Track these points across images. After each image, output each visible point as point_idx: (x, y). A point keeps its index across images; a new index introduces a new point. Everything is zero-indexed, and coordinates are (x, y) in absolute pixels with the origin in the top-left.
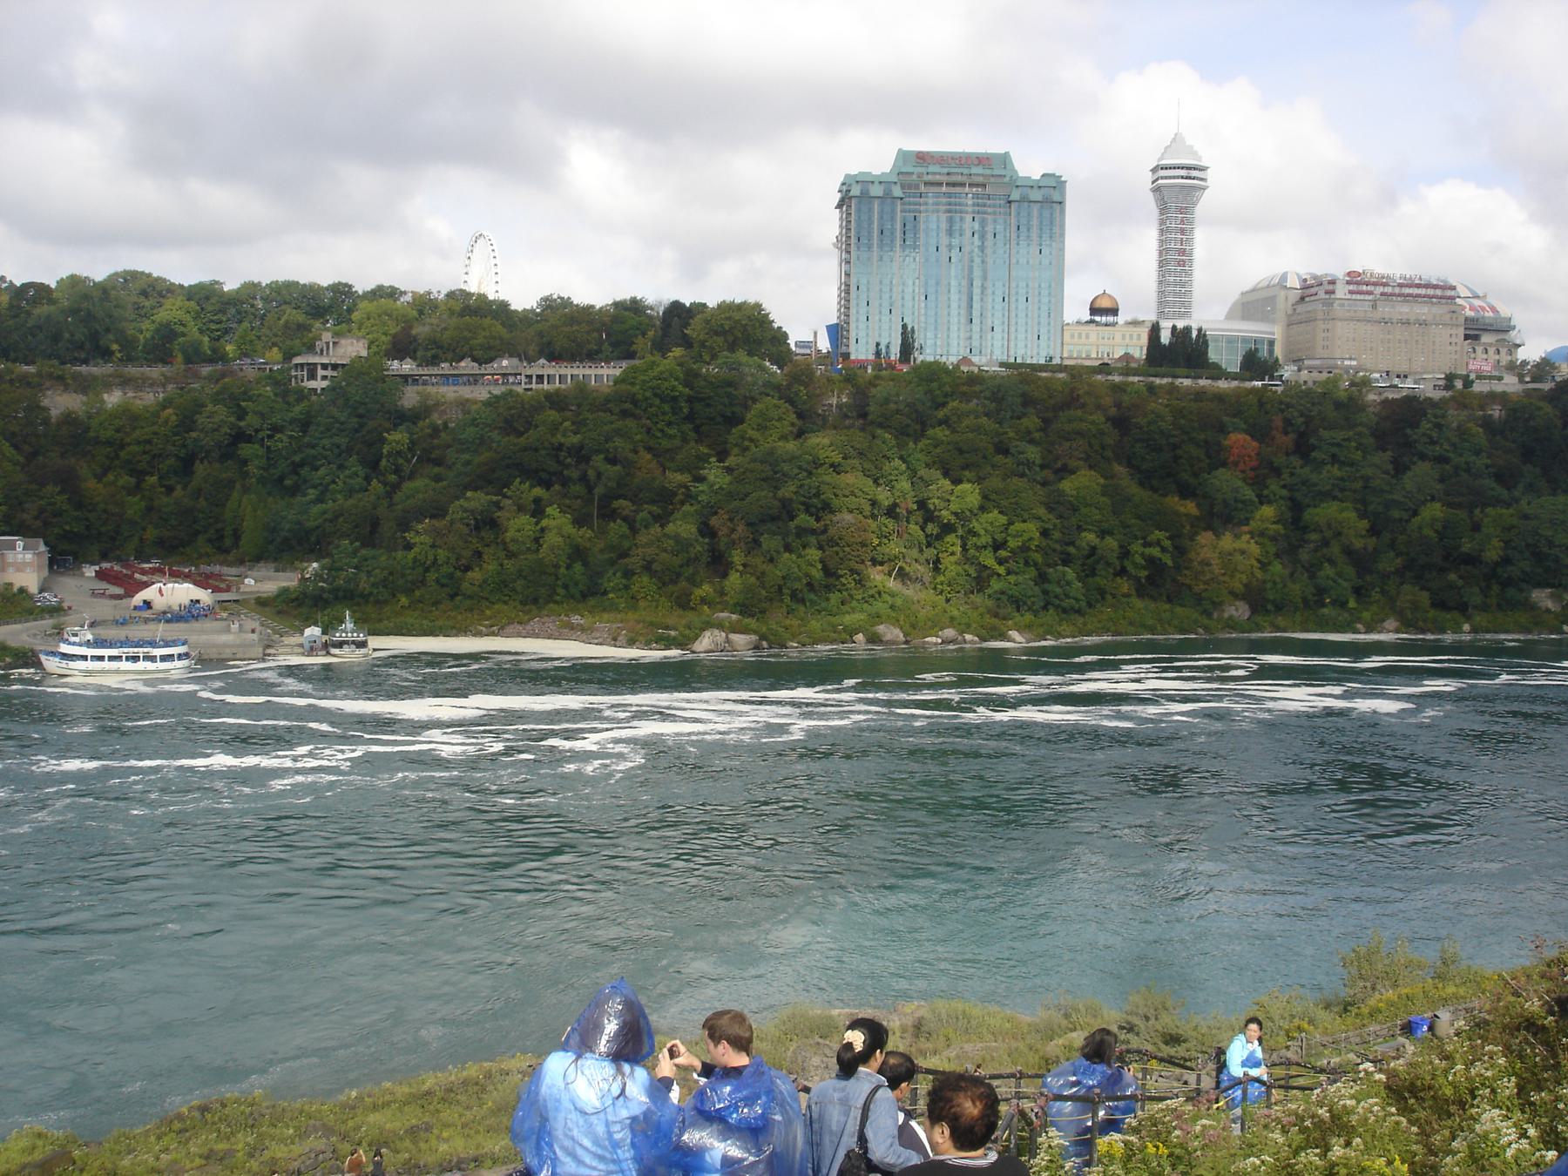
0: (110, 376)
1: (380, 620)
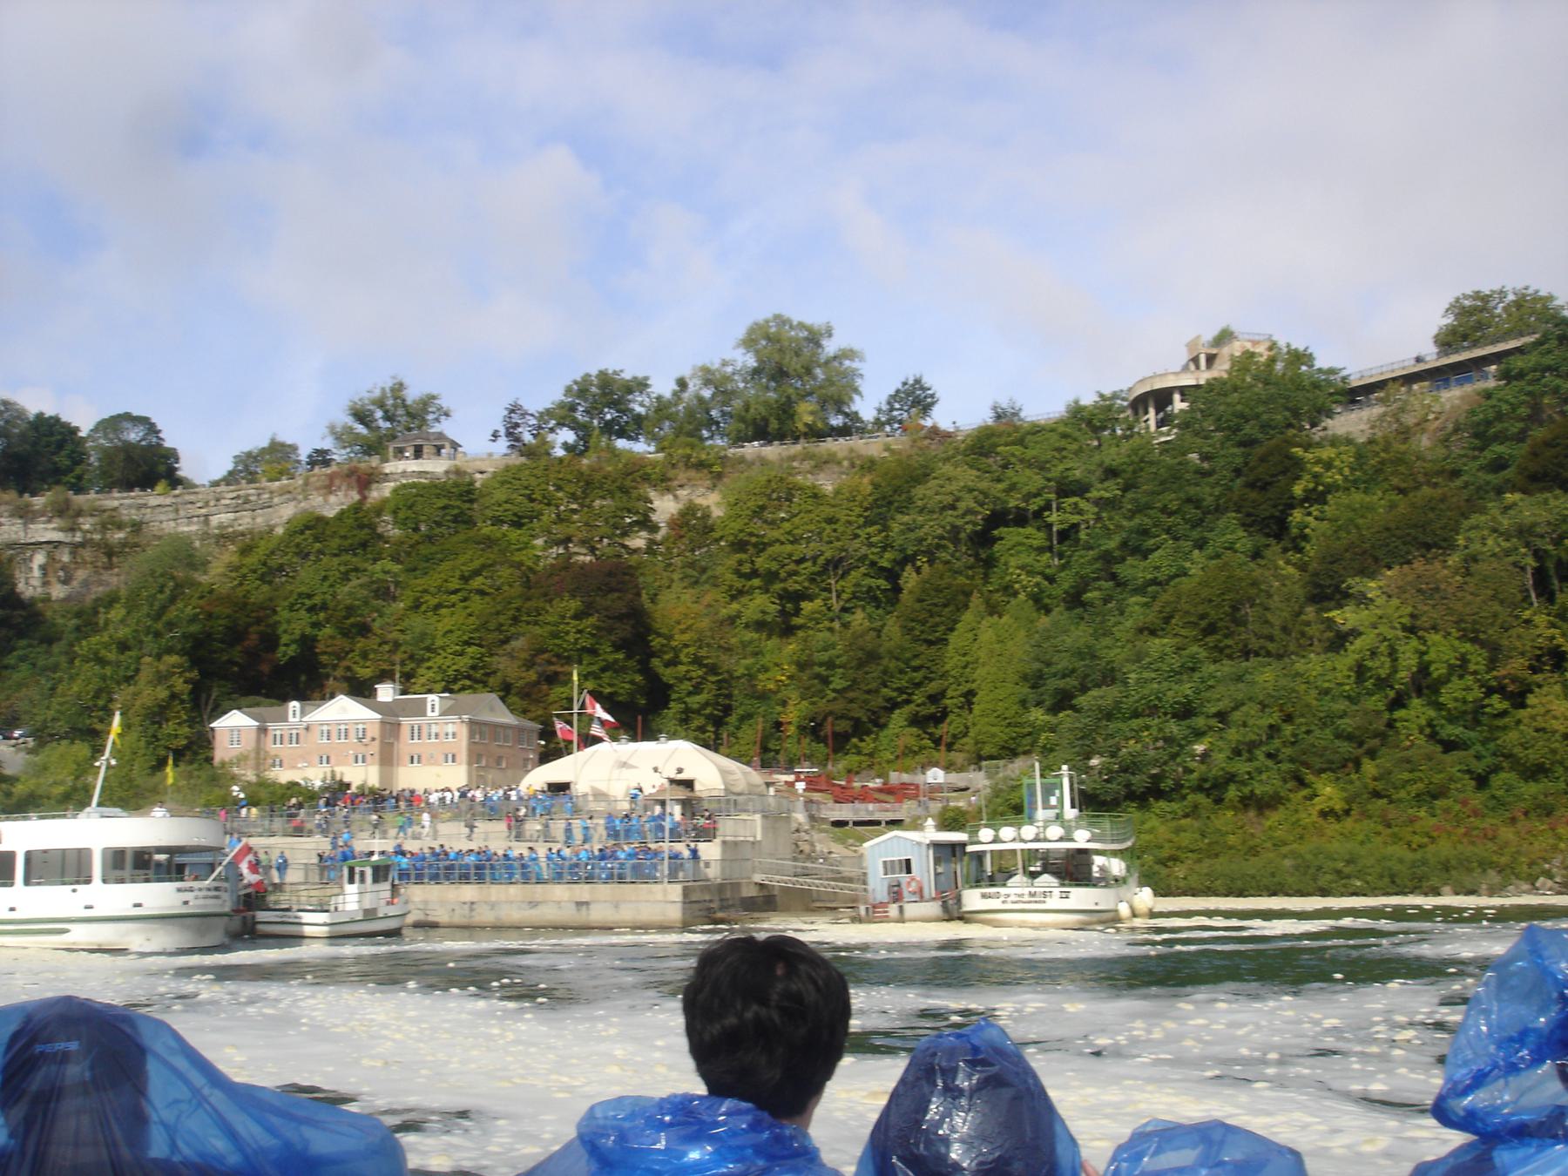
0: (793, 458)
1: (1254, 851)
